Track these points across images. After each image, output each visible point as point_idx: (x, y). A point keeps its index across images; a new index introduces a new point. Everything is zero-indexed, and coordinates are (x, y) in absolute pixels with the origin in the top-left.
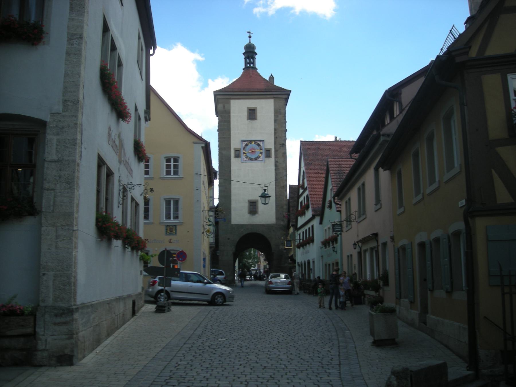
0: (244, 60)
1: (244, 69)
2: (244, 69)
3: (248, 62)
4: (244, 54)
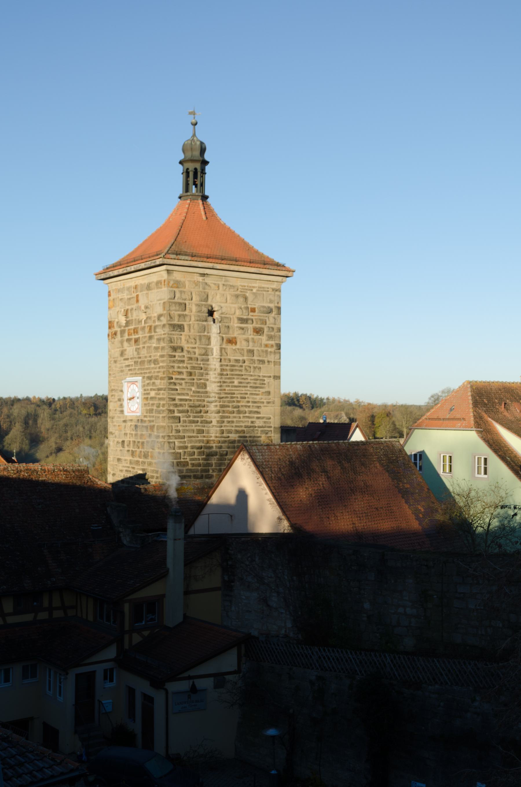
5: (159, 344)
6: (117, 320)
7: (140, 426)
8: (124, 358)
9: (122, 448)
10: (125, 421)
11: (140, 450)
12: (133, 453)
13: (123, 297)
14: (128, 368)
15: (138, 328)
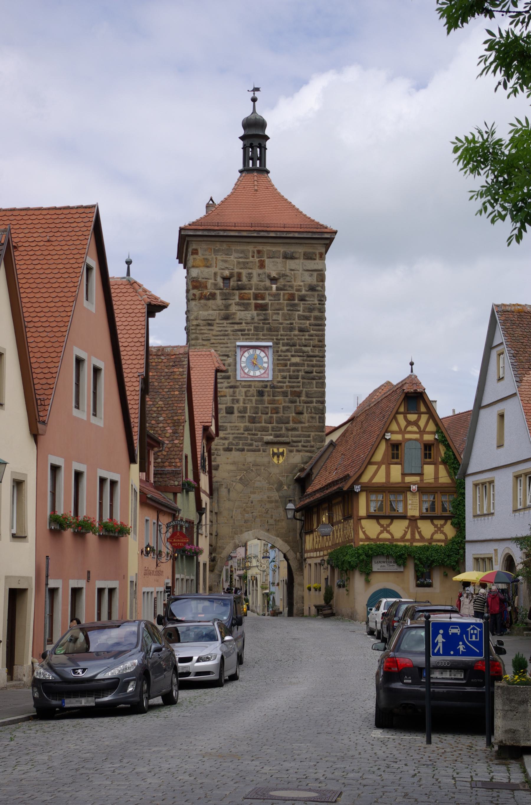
0: (241, 151)
1: (241, 172)
2: (241, 172)
3: (250, 153)
4: (242, 138)
6: (211, 281)
7: (268, 391)
9: (225, 415)
10: (231, 387)
11: (269, 415)
12: (253, 420)
13: (229, 259)
14: (240, 333)
15: (265, 293)
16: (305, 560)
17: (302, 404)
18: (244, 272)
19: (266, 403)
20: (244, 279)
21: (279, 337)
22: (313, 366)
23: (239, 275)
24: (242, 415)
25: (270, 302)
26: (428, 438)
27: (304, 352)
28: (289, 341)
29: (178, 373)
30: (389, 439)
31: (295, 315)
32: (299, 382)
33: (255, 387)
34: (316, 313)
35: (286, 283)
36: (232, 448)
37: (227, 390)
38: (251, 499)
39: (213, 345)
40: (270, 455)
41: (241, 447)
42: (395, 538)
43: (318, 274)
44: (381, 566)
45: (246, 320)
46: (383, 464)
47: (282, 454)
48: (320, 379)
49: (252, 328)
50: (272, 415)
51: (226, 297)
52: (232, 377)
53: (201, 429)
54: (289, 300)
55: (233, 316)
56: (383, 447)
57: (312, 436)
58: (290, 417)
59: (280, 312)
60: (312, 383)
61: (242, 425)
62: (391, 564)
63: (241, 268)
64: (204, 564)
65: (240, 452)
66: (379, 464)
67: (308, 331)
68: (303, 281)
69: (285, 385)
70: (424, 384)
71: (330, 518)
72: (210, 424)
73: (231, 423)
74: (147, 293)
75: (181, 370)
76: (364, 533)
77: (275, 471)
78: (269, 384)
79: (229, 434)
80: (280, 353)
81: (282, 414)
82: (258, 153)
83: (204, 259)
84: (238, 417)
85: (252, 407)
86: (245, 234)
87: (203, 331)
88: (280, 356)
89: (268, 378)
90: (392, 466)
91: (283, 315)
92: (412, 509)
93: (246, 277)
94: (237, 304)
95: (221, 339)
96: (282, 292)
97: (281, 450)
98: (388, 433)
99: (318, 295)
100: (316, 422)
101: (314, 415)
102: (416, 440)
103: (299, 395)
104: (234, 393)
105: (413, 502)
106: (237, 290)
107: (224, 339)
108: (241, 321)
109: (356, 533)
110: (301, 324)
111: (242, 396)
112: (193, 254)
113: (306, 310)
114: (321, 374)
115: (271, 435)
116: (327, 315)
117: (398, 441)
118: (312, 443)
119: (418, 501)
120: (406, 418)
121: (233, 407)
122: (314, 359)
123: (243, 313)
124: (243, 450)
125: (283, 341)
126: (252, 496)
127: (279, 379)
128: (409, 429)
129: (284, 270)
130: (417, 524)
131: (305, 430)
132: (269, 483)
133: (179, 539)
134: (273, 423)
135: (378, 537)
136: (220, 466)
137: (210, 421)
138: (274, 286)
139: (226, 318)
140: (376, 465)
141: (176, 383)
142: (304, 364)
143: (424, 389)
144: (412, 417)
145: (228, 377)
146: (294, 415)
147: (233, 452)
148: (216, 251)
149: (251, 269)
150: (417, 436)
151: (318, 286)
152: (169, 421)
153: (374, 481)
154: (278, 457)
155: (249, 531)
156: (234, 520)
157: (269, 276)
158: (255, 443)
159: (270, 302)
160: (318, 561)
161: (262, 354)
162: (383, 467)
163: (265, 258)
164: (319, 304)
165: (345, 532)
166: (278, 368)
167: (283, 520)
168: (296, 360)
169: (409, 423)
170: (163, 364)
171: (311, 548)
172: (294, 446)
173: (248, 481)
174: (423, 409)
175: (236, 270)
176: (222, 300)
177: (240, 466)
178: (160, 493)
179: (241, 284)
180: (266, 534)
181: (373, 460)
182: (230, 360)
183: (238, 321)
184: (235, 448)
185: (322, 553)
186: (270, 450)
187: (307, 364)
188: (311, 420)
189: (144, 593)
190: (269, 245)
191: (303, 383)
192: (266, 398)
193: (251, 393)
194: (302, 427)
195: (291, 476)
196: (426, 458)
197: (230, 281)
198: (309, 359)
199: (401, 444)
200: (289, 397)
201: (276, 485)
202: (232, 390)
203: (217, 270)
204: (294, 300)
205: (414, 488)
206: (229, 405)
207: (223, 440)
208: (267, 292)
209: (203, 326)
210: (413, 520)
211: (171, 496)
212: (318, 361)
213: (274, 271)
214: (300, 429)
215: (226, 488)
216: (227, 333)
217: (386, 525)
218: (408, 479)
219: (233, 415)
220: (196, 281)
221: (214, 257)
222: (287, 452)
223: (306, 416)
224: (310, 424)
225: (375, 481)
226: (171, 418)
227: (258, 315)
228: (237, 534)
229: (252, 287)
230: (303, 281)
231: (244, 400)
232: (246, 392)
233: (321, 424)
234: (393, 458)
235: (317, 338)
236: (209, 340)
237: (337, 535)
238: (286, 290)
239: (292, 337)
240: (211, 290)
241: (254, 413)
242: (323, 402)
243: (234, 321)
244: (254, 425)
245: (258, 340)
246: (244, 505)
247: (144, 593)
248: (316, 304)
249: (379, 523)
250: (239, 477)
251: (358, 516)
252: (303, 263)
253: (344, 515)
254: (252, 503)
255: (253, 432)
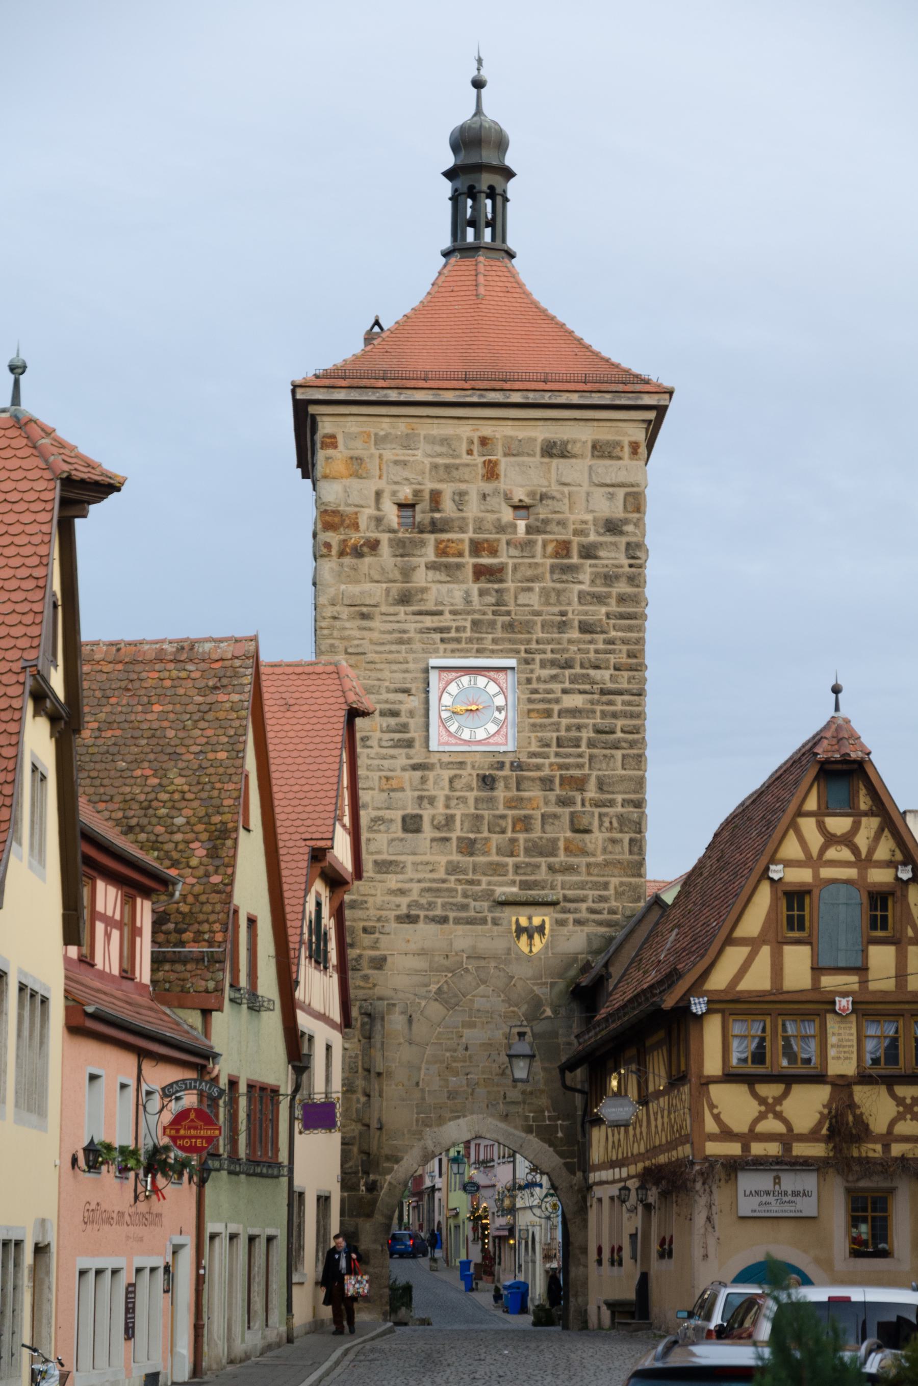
0: (449, 204)
2: (446, 254)
3: (469, 211)
4: (450, 174)
5: (610, 586)
6: (371, 511)
7: (505, 778)
8: (415, 608)
9: (400, 834)
10: (415, 767)
11: (509, 834)
12: (468, 847)
13: (411, 459)
14: (437, 636)
15: (498, 540)
16: (589, 1188)
17: (588, 808)
18: (448, 490)
19: (501, 806)
20: (448, 505)
21: (534, 646)
22: (614, 715)
23: (436, 497)
24: (443, 835)
25: (511, 562)
26: (880, 876)
27: (594, 683)
28: (558, 656)
29: (228, 705)
30: (780, 879)
31: (571, 592)
32: (580, 756)
33: (473, 767)
34: (622, 587)
35: (550, 516)
36: (418, 916)
37: (407, 775)
38: (464, 1040)
39: (373, 666)
40: (511, 932)
41: (438, 912)
42: (796, 1131)
43: (627, 495)
44: (760, 1204)
45: (452, 605)
46: (765, 942)
47: (541, 929)
48: (631, 747)
49: (468, 625)
50: (515, 835)
51: (403, 548)
52: (417, 744)
53: (306, 857)
54: (557, 555)
55: (419, 597)
56: (763, 899)
57: (612, 887)
58: (558, 839)
59: (537, 586)
60: (612, 756)
61: (443, 860)
62: (785, 1199)
63: (441, 481)
64: (319, 1198)
65: (439, 926)
66: (754, 944)
67: (603, 632)
68: (592, 511)
69: (547, 761)
70: (867, 740)
71: (642, 1085)
72: (329, 843)
73: (414, 854)
74: (66, 451)
75: (235, 697)
76: (717, 1118)
77: (521, 971)
78: (507, 760)
79: (411, 880)
80: (534, 685)
81: (539, 834)
82: (489, 209)
83: (351, 458)
84: (433, 840)
85: (467, 815)
86: (449, 396)
87: (347, 633)
88: (535, 691)
89: (506, 744)
90: (787, 949)
91: (545, 592)
92: (839, 1058)
93: (454, 501)
94: (431, 566)
95: (391, 652)
96: (540, 538)
97: (537, 921)
98: (776, 864)
99: (628, 544)
100: (623, 853)
101: (619, 835)
102: (847, 882)
103: (580, 784)
104: (424, 780)
105: (839, 1040)
106: (432, 532)
107: (398, 652)
108: (440, 608)
109: (698, 1118)
110: (586, 613)
111: (443, 789)
112: (324, 446)
113: (598, 581)
114: (636, 736)
115: (513, 883)
116: (649, 591)
117: (802, 884)
118: (614, 904)
119: (854, 1038)
120: (821, 827)
121: (420, 817)
122: (619, 699)
123: (444, 588)
124: (444, 920)
125: (543, 656)
126: (467, 1032)
127: (534, 748)
128: (832, 853)
129: (546, 483)
130: (851, 1095)
131: (596, 871)
132: (508, 1001)
133: (196, 1128)
134: (518, 856)
135: (751, 1130)
136: (389, 959)
137: (329, 835)
138: (521, 525)
139: (405, 599)
140: (746, 945)
141: (221, 731)
142: (594, 712)
143: (869, 754)
144: (839, 825)
145: (409, 744)
146: (569, 834)
147: (421, 926)
148: (380, 440)
149: (465, 481)
150: (851, 873)
151: (626, 522)
152: (200, 827)
153: (741, 987)
154: (531, 937)
155: (458, 1117)
156: (423, 1091)
157: (507, 498)
158: (473, 904)
159: (511, 562)
160: (614, 1190)
161: (493, 688)
162: (766, 951)
163: (498, 456)
164: (631, 566)
165: (672, 1116)
166: (532, 721)
167: (542, 1091)
168: (575, 701)
169: (831, 840)
170: (190, 683)
171: (601, 1160)
172: (569, 911)
173: (456, 996)
174: (864, 802)
175: (429, 486)
176: (397, 556)
177: (436, 959)
178: (168, 1011)
179: (441, 518)
180: (502, 1125)
181: (739, 933)
182: (413, 702)
183: (435, 608)
184: (426, 917)
185: (624, 1173)
186: (510, 921)
187: (602, 712)
188: (610, 848)
189: (82, 1273)
190: (510, 423)
191: (591, 757)
192: (500, 793)
193: (464, 781)
194: (588, 865)
195: (561, 985)
196: (874, 927)
197: (414, 511)
198: (605, 698)
199: (809, 892)
200: (558, 791)
201: (524, 1008)
202: (418, 774)
203: (382, 484)
204: (568, 555)
205: (844, 1003)
206: (410, 811)
207: (396, 895)
208: (504, 538)
209: (348, 620)
210: (842, 1085)
211: (194, 1018)
212: (629, 704)
213: (522, 486)
214: (584, 869)
215: (402, 1013)
216: (405, 636)
217: (774, 1098)
218: (828, 982)
219: (420, 835)
220: (333, 512)
221: (377, 453)
222: (551, 925)
223: (597, 838)
224: (608, 857)
225: (745, 985)
226: (206, 820)
227: (482, 593)
228: (430, 1126)
229: (467, 525)
230: (592, 511)
231: (448, 798)
232: (451, 781)
233: (636, 857)
234: (791, 927)
235: (625, 648)
236: (365, 654)
237: (656, 1127)
238: (550, 533)
239: (565, 645)
240: (368, 534)
241: (472, 832)
242: (639, 804)
243: (423, 608)
244: (471, 859)
245: (480, 652)
246: (448, 1054)
247: (82, 1273)
248: (622, 567)
249: (754, 1094)
250: (434, 988)
251: (700, 1076)
252: (590, 467)
253: (670, 1075)
254: (466, 1049)
255: (470, 876)
